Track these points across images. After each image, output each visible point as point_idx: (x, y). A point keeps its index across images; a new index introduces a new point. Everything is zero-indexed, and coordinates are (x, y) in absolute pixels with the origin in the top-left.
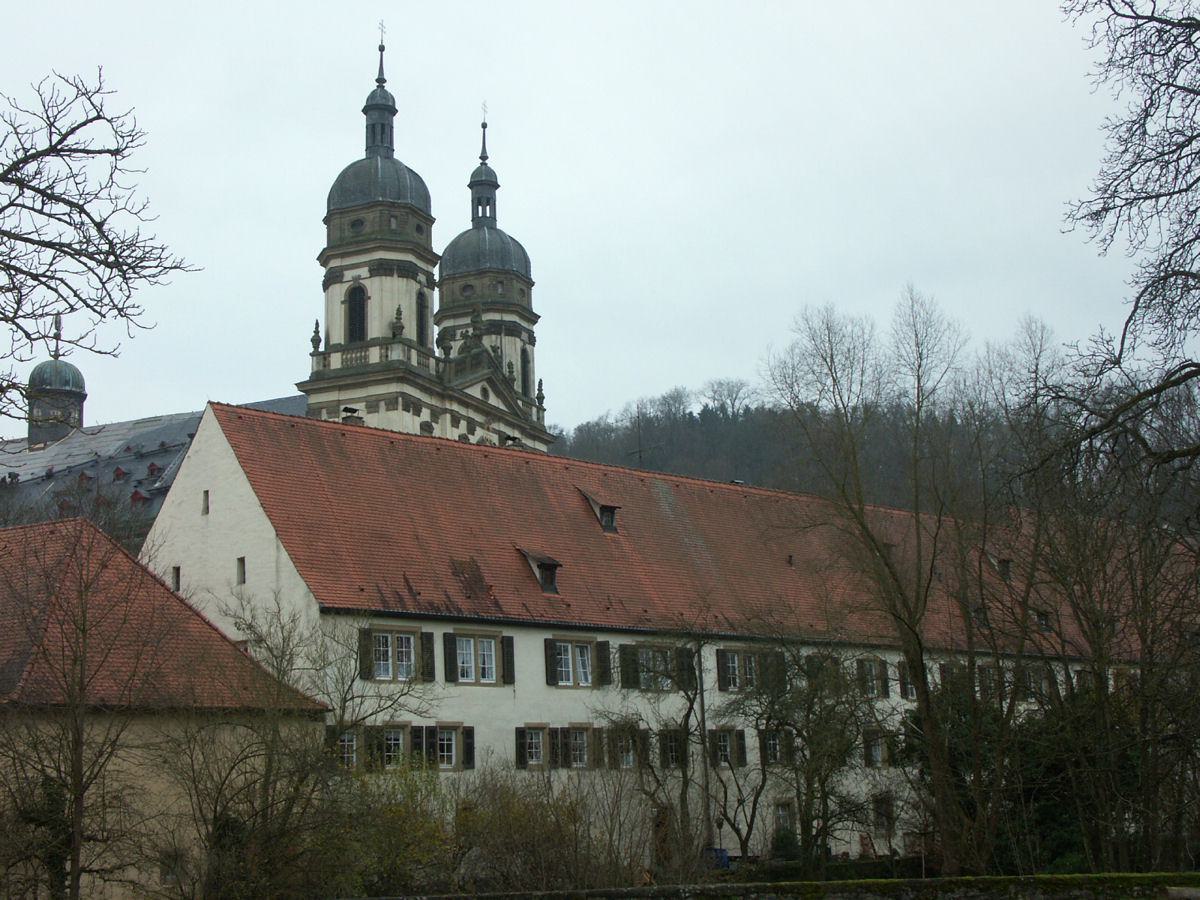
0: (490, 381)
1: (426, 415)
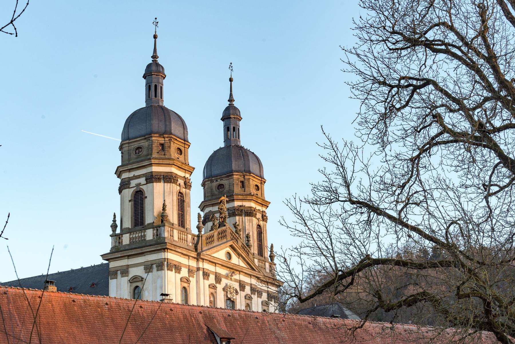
0: (231, 246)
1: (184, 272)
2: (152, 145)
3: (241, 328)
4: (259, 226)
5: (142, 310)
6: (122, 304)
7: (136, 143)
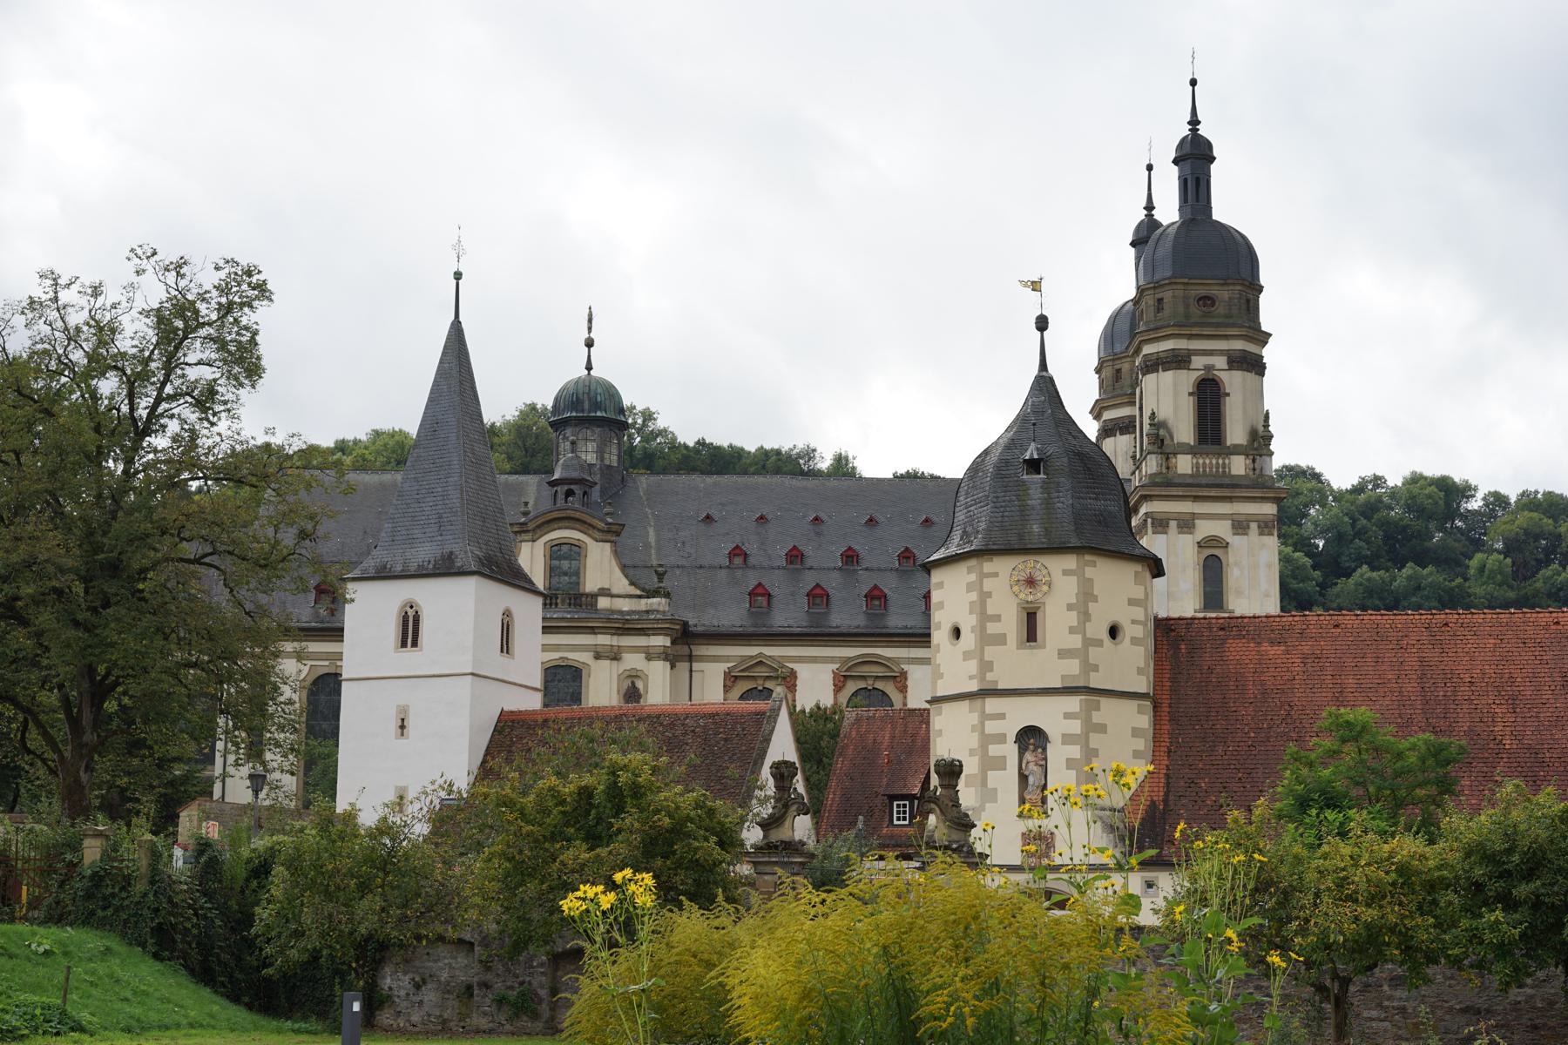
7: (1201, 287)
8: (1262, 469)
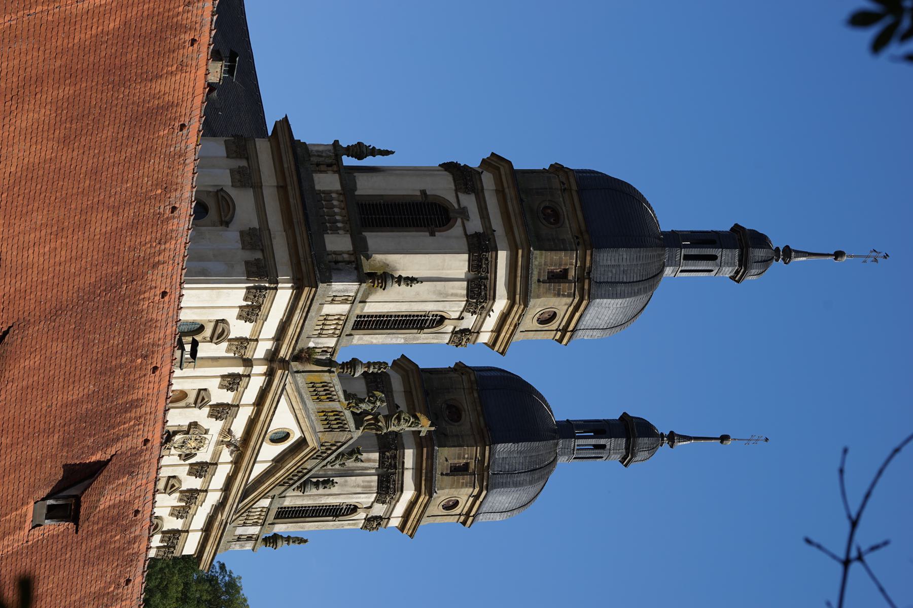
1: (240, 329)
2: (565, 250)
3: (103, 544)
4: (354, 509)
5: (157, 298)
6: (172, 247)
8: (339, 269)
